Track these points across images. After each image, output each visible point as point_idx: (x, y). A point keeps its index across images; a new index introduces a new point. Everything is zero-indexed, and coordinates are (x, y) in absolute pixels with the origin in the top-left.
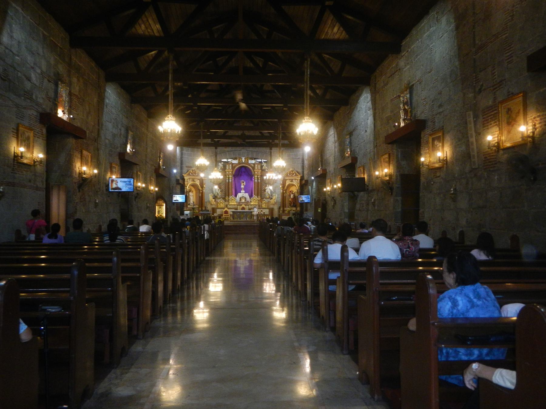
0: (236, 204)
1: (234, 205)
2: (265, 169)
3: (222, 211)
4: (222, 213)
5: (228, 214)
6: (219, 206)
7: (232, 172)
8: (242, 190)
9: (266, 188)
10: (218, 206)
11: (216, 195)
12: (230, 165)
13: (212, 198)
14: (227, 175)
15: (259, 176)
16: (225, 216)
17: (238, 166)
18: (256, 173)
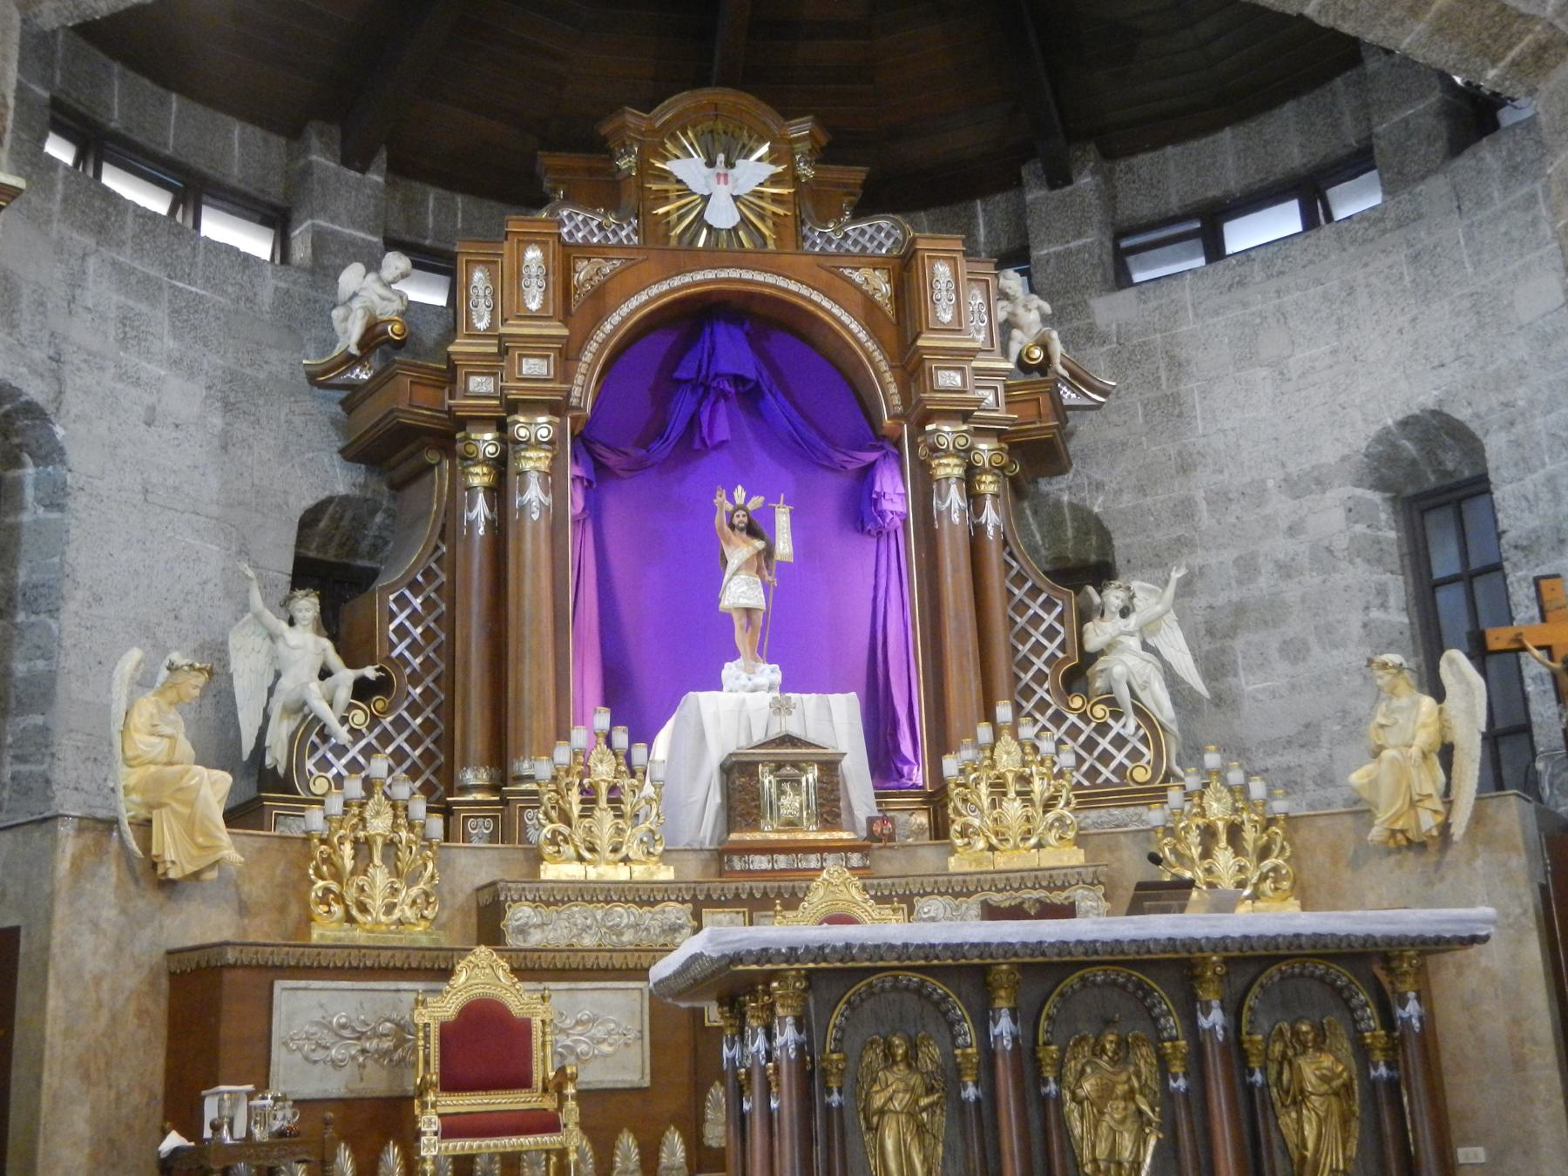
0: (666, 874)
1: (645, 896)
2: (1045, 366)
3: (403, 1031)
4: (397, 1058)
5: (522, 1081)
6: (327, 929)
7: (567, 356)
8: (734, 655)
9: (1092, 643)
10: (309, 919)
11: (277, 756)
12: (533, 255)
13: (185, 748)
14: (483, 422)
15: (985, 449)
16: (453, 1127)
17: (654, 290)
18: (949, 379)
